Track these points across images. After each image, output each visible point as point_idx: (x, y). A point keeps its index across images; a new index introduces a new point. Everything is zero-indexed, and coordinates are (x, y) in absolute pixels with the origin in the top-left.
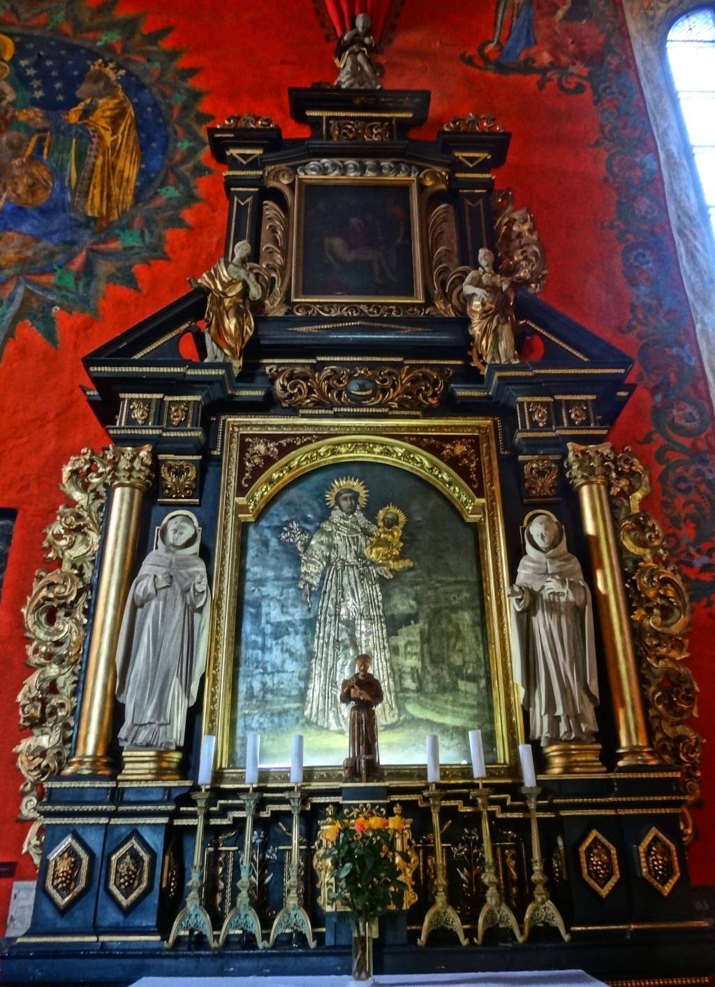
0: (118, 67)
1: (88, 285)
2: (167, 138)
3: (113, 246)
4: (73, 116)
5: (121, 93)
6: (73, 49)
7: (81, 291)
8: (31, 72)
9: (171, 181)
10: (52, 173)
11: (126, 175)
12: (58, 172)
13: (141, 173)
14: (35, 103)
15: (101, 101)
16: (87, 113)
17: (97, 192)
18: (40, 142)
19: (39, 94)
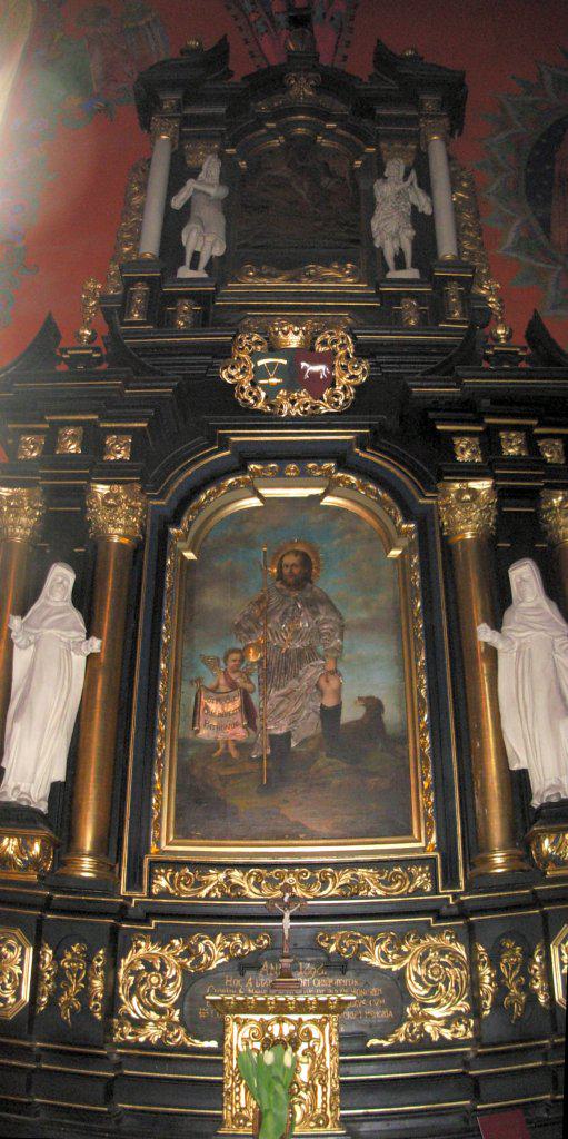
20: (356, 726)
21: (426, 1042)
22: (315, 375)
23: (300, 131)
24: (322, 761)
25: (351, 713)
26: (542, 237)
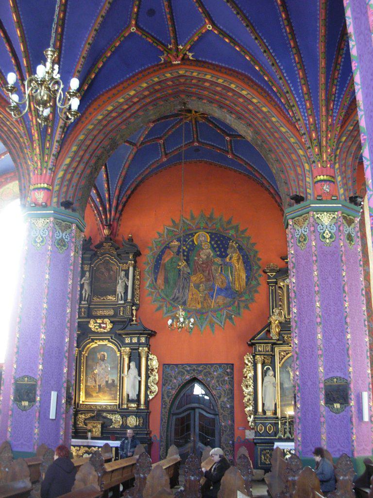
0: (236, 243)
1: (239, 309)
2: (251, 265)
3: (243, 299)
4: (227, 260)
5: (238, 252)
6: (224, 237)
7: (238, 311)
8: (215, 246)
9: (254, 279)
10: (226, 277)
11: (243, 277)
12: (227, 277)
13: (247, 277)
14: (218, 256)
15: (234, 255)
16: (231, 258)
17: (237, 283)
18: (222, 268)
19: (218, 253)
20: (111, 384)
21: (115, 428)
22: (104, 327)
23: (108, 258)
24: (106, 388)
25: (110, 382)
26: (155, 283)
